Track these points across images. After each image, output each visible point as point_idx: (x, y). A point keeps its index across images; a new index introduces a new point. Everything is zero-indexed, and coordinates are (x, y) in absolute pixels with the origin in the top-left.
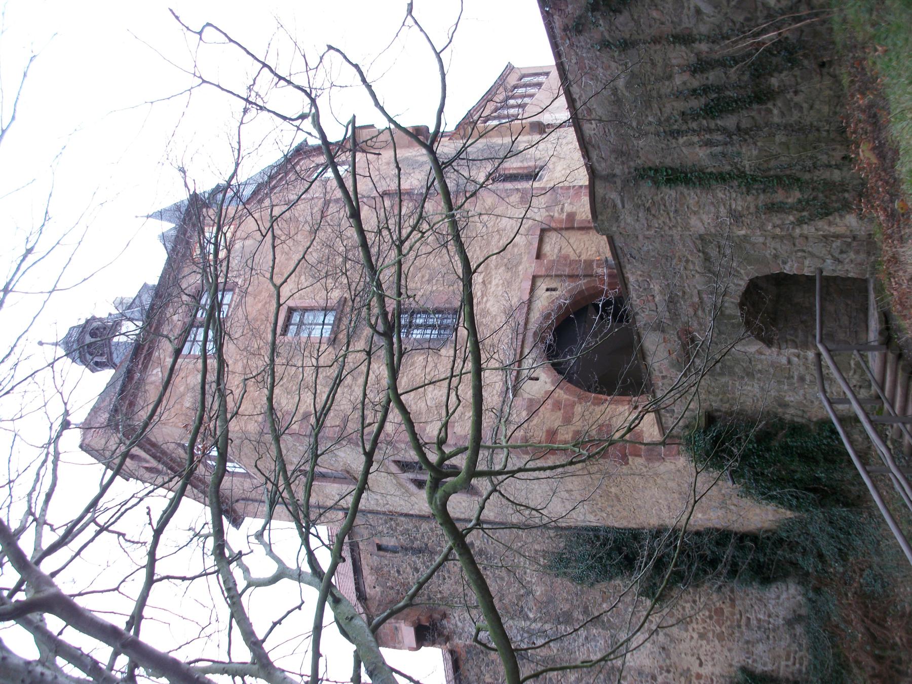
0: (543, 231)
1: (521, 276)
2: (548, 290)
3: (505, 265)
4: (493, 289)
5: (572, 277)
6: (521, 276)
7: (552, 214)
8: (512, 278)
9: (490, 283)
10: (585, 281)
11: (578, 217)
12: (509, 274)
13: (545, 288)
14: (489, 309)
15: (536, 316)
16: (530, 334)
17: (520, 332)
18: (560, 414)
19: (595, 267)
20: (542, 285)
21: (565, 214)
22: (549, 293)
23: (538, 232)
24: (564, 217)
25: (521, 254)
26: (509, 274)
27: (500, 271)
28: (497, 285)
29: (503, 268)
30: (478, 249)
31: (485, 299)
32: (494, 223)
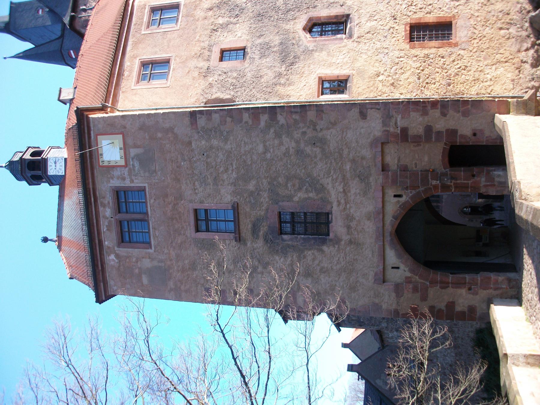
0: (383, 144)
1: (373, 187)
2: (395, 196)
3: (359, 176)
4: (352, 198)
5: (413, 187)
6: (373, 187)
7: (388, 129)
8: (366, 188)
9: (349, 191)
10: (423, 189)
11: (411, 133)
12: (363, 183)
13: (393, 194)
14: (353, 215)
15: (389, 219)
16: (387, 234)
17: (381, 234)
18: (418, 295)
19: (430, 180)
20: (390, 192)
21: (399, 128)
22: (397, 199)
23: (380, 145)
24: (399, 132)
25: (369, 167)
26: (363, 183)
27: (355, 182)
28: (355, 193)
29: (357, 179)
30: (333, 161)
31: (348, 206)
32: (342, 137)
